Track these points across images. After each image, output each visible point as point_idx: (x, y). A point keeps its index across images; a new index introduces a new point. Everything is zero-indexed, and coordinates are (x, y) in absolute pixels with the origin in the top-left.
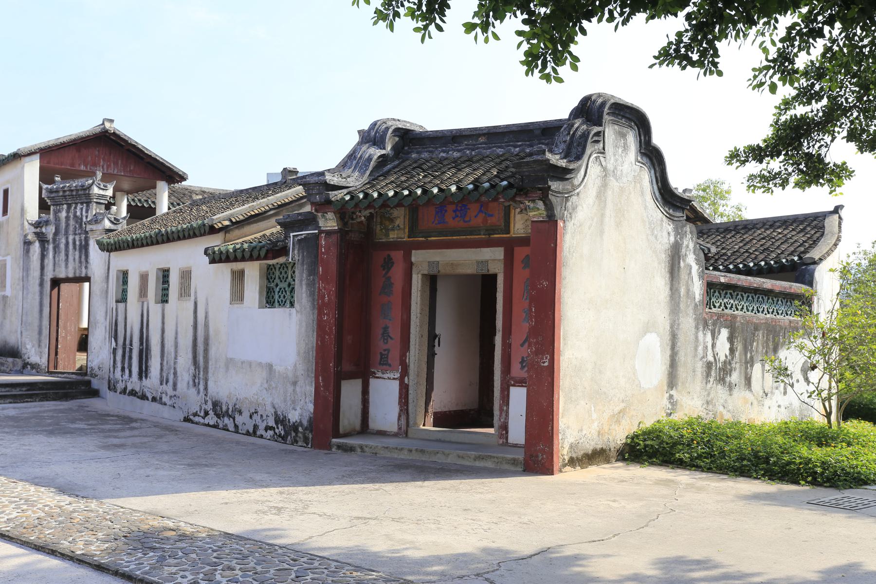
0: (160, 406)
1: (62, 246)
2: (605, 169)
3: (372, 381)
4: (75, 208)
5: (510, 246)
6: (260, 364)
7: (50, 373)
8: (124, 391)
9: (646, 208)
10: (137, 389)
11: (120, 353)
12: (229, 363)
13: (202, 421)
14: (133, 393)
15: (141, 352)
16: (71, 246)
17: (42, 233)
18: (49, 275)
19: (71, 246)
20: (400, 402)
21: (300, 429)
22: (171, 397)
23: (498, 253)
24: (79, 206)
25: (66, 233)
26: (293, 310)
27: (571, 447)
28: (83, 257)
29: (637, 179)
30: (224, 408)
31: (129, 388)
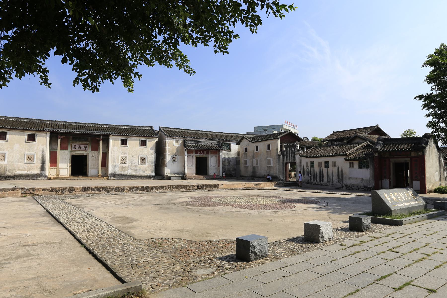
0: (328, 187)
1: (288, 156)
2: (430, 145)
3: (383, 181)
4: (291, 149)
5: (412, 158)
6: (359, 178)
7: (287, 181)
8: (315, 184)
9: (435, 151)
10: (320, 183)
11: (312, 178)
12: (349, 178)
13: (342, 188)
14: (318, 184)
15: (320, 177)
16: (290, 156)
17: (284, 154)
18: (285, 162)
19: (290, 156)
20: (389, 184)
21: (371, 188)
22: (331, 185)
23: (409, 159)
24: (292, 149)
25: (289, 154)
26: (368, 169)
27: (428, 190)
28: (294, 158)
29: (434, 146)
30: (349, 186)
31: (316, 183)
